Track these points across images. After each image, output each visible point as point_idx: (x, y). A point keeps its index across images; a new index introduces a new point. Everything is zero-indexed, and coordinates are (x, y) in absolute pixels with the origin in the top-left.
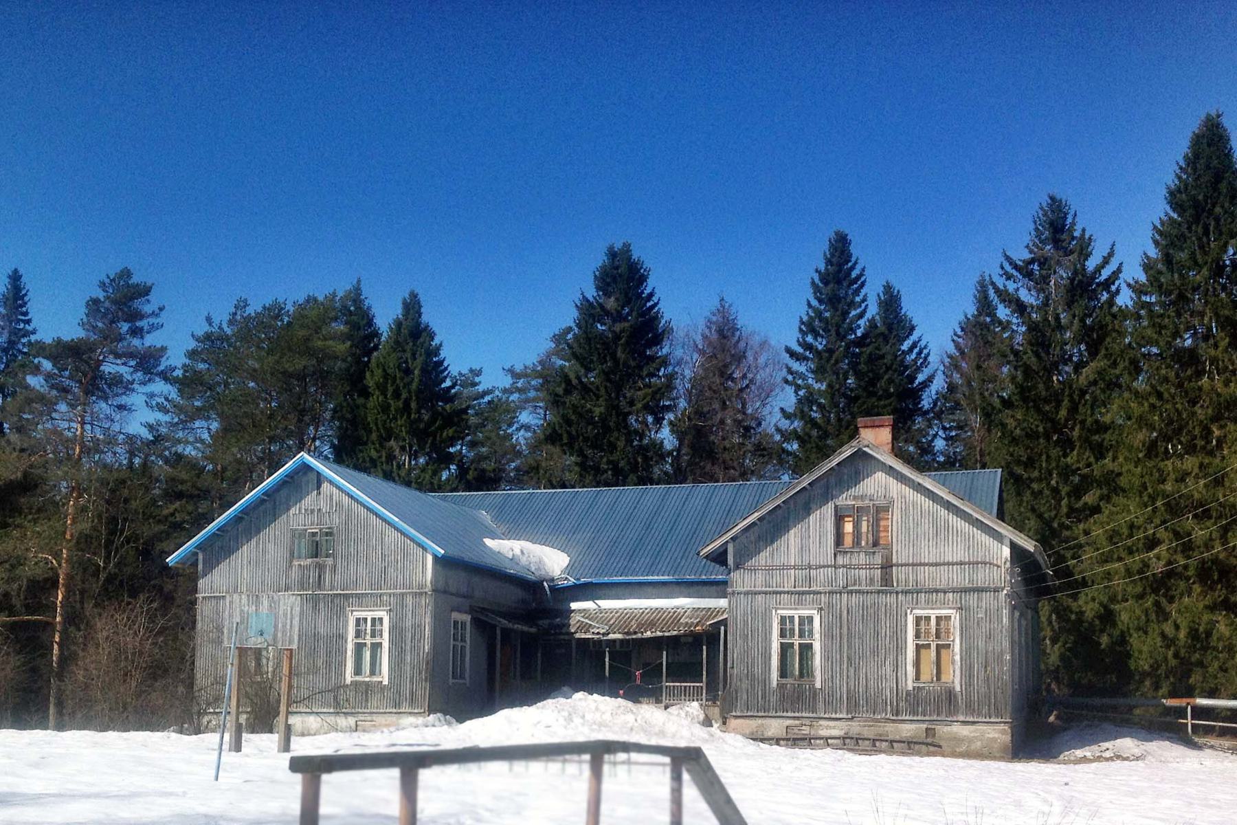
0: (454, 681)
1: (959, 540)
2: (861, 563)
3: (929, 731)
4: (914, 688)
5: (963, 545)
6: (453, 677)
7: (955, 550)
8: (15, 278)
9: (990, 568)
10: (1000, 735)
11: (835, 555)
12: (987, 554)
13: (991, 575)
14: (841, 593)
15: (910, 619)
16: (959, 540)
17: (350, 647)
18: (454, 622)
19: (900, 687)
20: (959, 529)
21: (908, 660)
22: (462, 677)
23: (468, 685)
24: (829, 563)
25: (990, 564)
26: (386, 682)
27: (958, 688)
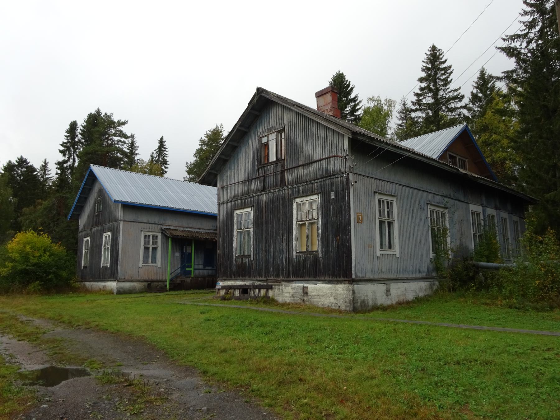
0: (144, 265)
1: (319, 144)
2: (271, 172)
3: (305, 289)
4: (296, 256)
5: (321, 146)
6: (146, 260)
7: (317, 151)
8: (162, 142)
9: (337, 159)
10: (345, 292)
11: (258, 170)
12: (335, 149)
13: (338, 165)
14: (262, 195)
15: (294, 206)
16: (319, 144)
17: (103, 250)
18: (145, 236)
19: (290, 257)
20: (319, 135)
21: (294, 237)
22: (154, 260)
23: (159, 266)
24: (256, 177)
25: (337, 157)
26: (109, 266)
27: (320, 255)
